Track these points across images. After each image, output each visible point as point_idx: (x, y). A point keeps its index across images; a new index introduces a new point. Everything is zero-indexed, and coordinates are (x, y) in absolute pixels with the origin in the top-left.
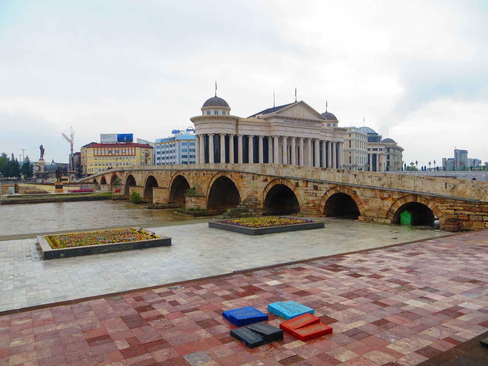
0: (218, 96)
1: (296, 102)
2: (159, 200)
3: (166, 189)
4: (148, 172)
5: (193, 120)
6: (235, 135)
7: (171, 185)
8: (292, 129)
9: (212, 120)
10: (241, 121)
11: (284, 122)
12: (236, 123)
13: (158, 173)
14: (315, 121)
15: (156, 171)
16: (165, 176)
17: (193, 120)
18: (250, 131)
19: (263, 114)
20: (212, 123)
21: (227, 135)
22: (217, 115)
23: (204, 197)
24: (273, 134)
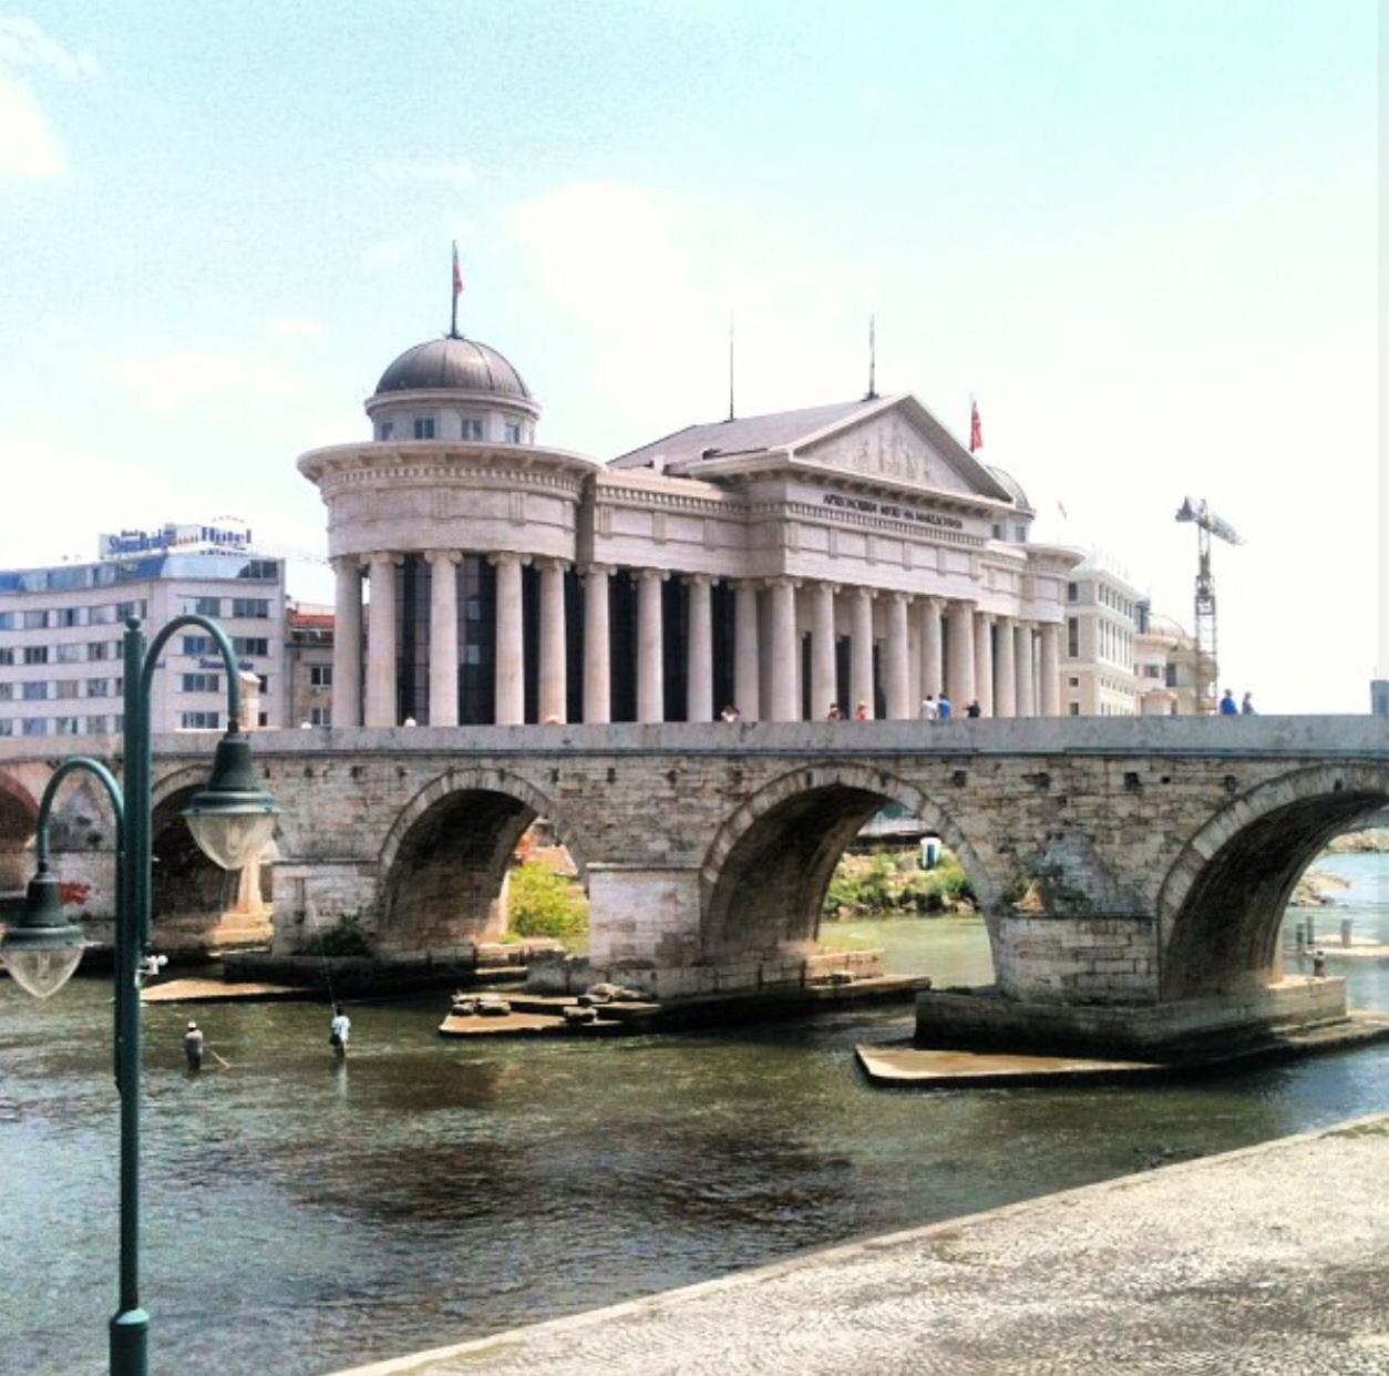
2: (632, 947)
3: (681, 876)
4: (442, 765)
5: (316, 468)
6: (573, 567)
7: (725, 847)
8: (858, 545)
10: (608, 488)
13: (581, 778)
15: (553, 764)
16: (666, 792)
17: (316, 468)
18: (650, 544)
21: (536, 558)
23: (1140, 918)
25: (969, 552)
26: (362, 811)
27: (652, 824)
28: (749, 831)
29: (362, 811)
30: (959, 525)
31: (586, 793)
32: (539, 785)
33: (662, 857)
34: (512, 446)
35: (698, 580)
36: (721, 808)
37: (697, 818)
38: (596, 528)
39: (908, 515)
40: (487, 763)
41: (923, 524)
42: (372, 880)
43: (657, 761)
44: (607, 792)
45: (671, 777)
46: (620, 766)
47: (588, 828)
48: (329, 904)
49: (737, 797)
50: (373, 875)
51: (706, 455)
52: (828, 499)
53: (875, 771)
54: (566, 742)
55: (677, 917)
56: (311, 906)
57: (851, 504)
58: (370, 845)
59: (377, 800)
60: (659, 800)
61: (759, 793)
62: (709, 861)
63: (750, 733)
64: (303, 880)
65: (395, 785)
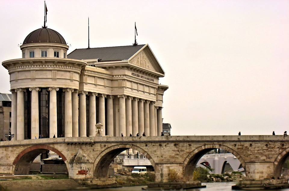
0: (49, 26)
2: (263, 176)
3: (271, 163)
4: (203, 143)
7: (279, 158)
9: (40, 66)
11: (132, 76)
12: (80, 72)
15: (235, 143)
16: (265, 148)
19: (99, 61)
20: (58, 70)
22: (58, 59)
27: (262, 154)
29: (178, 153)
30: (153, 81)
32: (231, 147)
33: (264, 160)
36: (279, 150)
37: (273, 153)
40: (215, 143)
41: (148, 80)
42: (182, 167)
43: (263, 143)
44: (250, 148)
45: (267, 145)
46: (253, 144)
47: (244, 155)
49: (283, 149)
50: (182, 166)
51: (99, 61)
52: (132, 74)
55: (270, 171)
58: (180, 160)
59: (182, 151)
60: (263, 150)
62: (276, 160)
64: (169, 167)
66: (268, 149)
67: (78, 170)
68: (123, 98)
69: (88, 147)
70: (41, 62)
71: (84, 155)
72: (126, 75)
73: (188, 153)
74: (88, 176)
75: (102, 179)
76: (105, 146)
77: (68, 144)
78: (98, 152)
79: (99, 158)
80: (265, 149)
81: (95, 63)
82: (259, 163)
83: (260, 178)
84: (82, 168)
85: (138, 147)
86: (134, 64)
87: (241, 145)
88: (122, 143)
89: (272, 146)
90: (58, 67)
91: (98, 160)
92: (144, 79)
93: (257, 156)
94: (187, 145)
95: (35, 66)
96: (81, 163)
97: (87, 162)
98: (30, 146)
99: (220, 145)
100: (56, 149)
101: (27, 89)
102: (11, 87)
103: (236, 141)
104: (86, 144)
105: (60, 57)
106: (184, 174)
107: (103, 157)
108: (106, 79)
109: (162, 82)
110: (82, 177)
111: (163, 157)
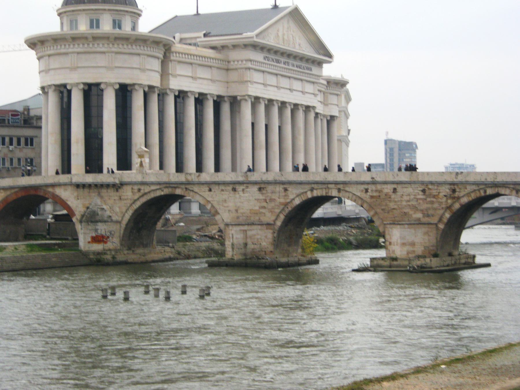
1: (276, 7)
2: (414, 251)
3: (431, 226)
4: (308, 187)
7: (447, 215)
11: (264, 61)
12: (161, 56)
14: (302, 58)
16: (421, 196)
18: (191, 80)
19: (205, 35)
20: (117, 53)
24: (237, 91)
25: (313, 83)
26: (265, 204)
27: (415, 208)
28: (458, 210)
29: (265, 204)
30: (311, 70)
31: (383, 196)
32: (359, 194)
33: (419, 219)
34: (133, 33)
35: (209, 97)
36: (446, 201)
37: (436, 205)
38: (170, 72)
39: (293, 66)
40: (330, 186)
41: (299, 69)
42: (271, 231)
43: (416, 186)
45: (424, 191)
46: (399, 188)
47: (383, 210)
48: (256, 240)
49: (454, 198)
50: (271, 229)
51: (205, 35)
52: (265, 58)
53: (514, 189)
54: (373, 178)
55: (429, 240)
56: (249, 242)
57: (273, 60)
58: (269, 218)
60: (417, 200)
61: (463, 197)
62: (440, 220)
63: (460, 176)
64: (246, 231)
65: (284, 194)
66: (426, 199)
67: (91, 235)
68: (246, 100)
69: (111, 192)
70: (86, 38)
71: (105, 207)
72: (251, 61)
73: (281, 204)
74: (109, 245)
75: (140, 251)
76: (139, 190)
77: (78, 186)
78: (129, 202)
79: (130, 212)
80: (420, 199)
81: (198, 40)
82: (406, 226)
83: (408, 253)
84: (99, 231)
85: (195, 192)
86: (270, 41)
87: (376, 191)
88: (168, 185)
89: (434, 192)
90: (116, 46)
91: (127, 217)
92: (291, 67)
93: (406, 211)
94: (281, 189)
95: (76, 46)
96: (97, 222)
97: (109, 220)
98: (16, 190)
99: (339, 190)
100: (57, 196)
101: (65, 86)
102: (41, 83)
103: (368, 183)
104: (108, 186)
105: (123, 27)
106: (277, 243)
107: (136, 211)
108: (214, 67)
109: (329, 71)
110: (98, 247)
111: (239, 212)
